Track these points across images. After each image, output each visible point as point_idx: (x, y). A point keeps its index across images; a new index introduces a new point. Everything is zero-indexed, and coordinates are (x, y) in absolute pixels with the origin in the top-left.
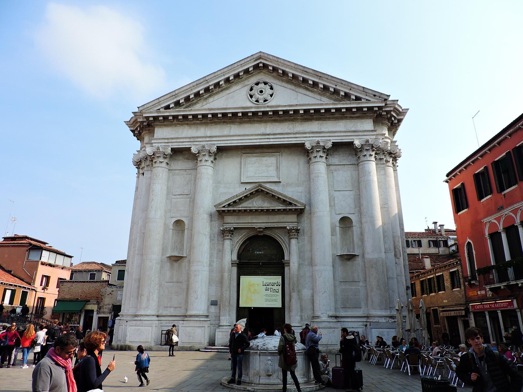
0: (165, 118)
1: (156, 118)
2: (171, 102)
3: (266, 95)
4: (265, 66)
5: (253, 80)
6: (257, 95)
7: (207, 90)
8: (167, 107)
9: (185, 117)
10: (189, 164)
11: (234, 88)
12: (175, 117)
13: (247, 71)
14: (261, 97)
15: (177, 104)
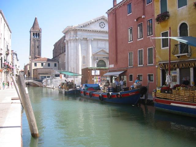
0: (81, 30)
1: (79, 30)
2: (82, 26)
3: (103, 26)
4: (104, 19)
5: (100, 21)
6: (101, 26)
7: (91, 23)
8: (81, 27)
9: (86, 30)
10: (86, 42)
11: (96, 23)
12: (84, 30)
13: (100, 19)
14: (102, 27)
15: (84, 26)
